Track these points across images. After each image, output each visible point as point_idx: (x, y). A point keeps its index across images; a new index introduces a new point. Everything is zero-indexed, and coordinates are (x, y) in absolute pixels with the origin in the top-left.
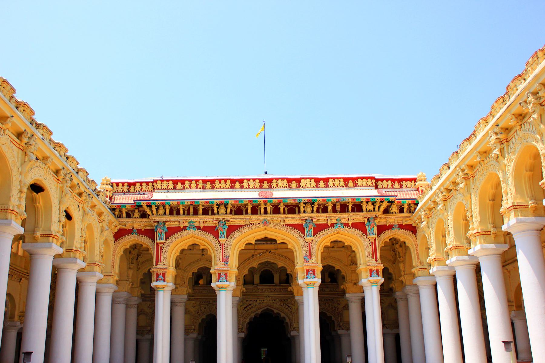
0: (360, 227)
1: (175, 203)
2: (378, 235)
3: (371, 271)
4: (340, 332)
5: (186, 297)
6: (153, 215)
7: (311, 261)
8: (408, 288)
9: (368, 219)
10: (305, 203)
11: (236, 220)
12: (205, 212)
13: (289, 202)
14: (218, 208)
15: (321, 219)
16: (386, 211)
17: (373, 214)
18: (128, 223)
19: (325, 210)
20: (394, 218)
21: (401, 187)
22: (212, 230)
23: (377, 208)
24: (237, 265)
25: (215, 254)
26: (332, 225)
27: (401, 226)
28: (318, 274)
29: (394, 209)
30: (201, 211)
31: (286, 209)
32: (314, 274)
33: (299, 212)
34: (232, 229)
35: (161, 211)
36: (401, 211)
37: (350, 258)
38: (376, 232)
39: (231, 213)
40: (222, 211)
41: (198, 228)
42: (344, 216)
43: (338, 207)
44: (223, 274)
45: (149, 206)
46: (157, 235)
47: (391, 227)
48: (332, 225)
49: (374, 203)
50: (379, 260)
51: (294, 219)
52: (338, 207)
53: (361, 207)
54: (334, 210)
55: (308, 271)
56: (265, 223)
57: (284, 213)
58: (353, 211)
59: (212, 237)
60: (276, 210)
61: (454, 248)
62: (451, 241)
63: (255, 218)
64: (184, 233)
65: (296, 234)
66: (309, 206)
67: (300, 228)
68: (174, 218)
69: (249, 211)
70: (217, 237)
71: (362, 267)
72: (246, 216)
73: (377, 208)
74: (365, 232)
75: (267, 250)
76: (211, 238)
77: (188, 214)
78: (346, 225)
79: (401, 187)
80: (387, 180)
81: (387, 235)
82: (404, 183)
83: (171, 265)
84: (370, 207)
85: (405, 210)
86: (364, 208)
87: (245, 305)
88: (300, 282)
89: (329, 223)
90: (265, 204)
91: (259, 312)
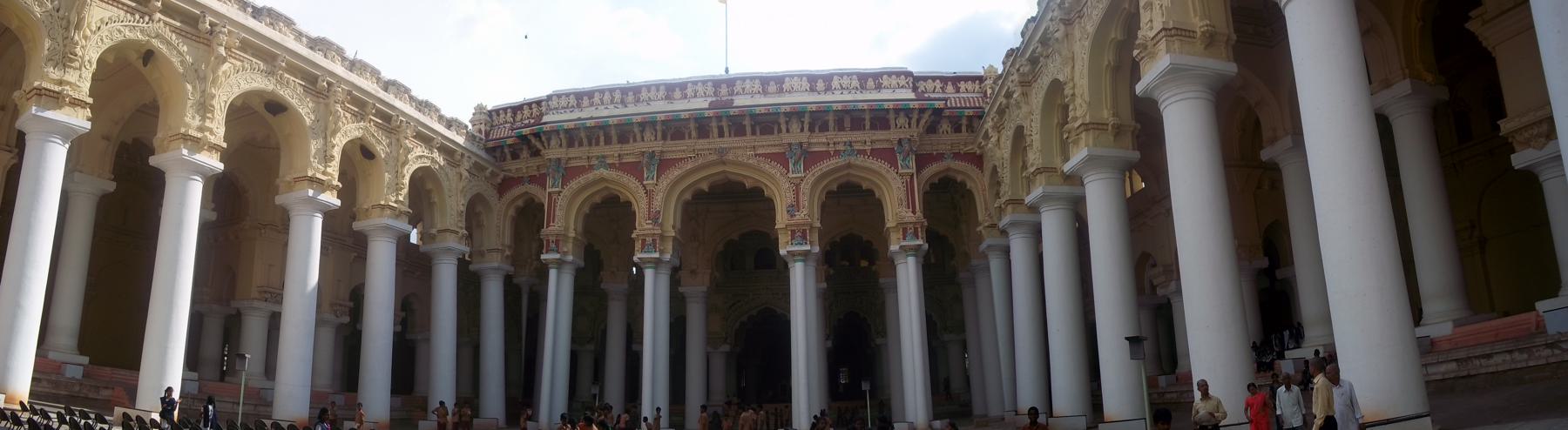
0: (888, 155)
1: (571, 125)
2: (919, 170)
3: (905, 231)
4: (879, 341)
5: (626, 286)
7: (801, 216)
8: (974, 262)
9: (900, 141)
10: (785, 114)
11: (675, 148)
12: (623, 139)
13: (758, 110)
14: (642, 132)
15: (819, 141)
16: (932, 129)
18: (514, 167)
19: (824, 128)
20: (946, 139)
21: (958, 91)
22: (635, 169)
23: (914, 121)
24: (678, 225)
25: (641, 208)
26: (837, 153)
27: (957, 156)
28: (816, 237)
29: (945, 126)
30: (615, 139)
32: (804, 237)
33: (780, 131)
34: (664, 165)
35: (553, 142)
36: (958, 129)
38: (913, 164)
40: (648, 135)
41: (612, 166)
42: (857, 136)
43: (847, 124)
44: (649, 240)
45: (537, 135)
46: (549, 182)
47: (940, 157)
48: (837, 153)
49: (908, 112)
50: (919, 214)
51: (768, 144)
52: (847, 124)
53: (888, 121)
54: (840, 126)
56: (722, 152)
57: (754, 133)
58: (873, 127)
59: (633, 179)
60: (739, 130)
61: (1039, 171)
62: (1034, 158)
63: (703, 144)
64: (591, 176)
65: (774, 170)
66: (794, 120)
67: (781, 159)
68: (573, 152)
69: (694, 134)
70: (641, 179)
71: (890, 223)
73: (914, 121)
74: (894, 164)
76: (630, 182)
77: (597, 144)
78: (862, 152)
79: (958, 91)
80: (934, 79)
81: (932, 169)
82: (962, 85)
83: (572, 226)
84: (902, 120)
85: (964, 128)
86: (892, 122)
88: (782, 252)
91: (754, 313)
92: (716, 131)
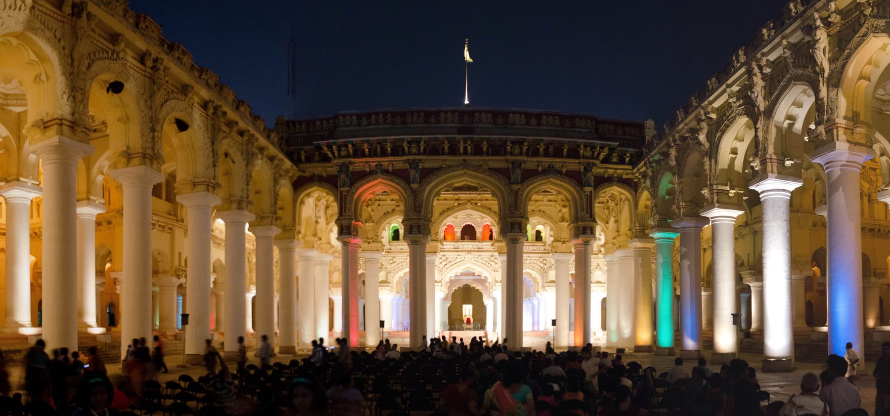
6: (335, 157)
14: (409, 147)
17: (591, 161)
19: (536, 153)
31: (490, 150)
37: (560, 214)
39: (424, 153)
43: (551, 149)
52: (551, 149)
55: (513, 224)
58: (568, 156)
72: (443, 157)
75: (469, 201)
78: (559, 172)
87: (444, 263)
89: (540, 169)
90: (465, 142)
92: (462, 150)
